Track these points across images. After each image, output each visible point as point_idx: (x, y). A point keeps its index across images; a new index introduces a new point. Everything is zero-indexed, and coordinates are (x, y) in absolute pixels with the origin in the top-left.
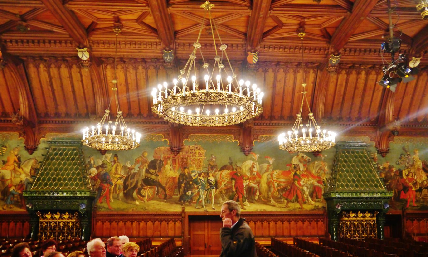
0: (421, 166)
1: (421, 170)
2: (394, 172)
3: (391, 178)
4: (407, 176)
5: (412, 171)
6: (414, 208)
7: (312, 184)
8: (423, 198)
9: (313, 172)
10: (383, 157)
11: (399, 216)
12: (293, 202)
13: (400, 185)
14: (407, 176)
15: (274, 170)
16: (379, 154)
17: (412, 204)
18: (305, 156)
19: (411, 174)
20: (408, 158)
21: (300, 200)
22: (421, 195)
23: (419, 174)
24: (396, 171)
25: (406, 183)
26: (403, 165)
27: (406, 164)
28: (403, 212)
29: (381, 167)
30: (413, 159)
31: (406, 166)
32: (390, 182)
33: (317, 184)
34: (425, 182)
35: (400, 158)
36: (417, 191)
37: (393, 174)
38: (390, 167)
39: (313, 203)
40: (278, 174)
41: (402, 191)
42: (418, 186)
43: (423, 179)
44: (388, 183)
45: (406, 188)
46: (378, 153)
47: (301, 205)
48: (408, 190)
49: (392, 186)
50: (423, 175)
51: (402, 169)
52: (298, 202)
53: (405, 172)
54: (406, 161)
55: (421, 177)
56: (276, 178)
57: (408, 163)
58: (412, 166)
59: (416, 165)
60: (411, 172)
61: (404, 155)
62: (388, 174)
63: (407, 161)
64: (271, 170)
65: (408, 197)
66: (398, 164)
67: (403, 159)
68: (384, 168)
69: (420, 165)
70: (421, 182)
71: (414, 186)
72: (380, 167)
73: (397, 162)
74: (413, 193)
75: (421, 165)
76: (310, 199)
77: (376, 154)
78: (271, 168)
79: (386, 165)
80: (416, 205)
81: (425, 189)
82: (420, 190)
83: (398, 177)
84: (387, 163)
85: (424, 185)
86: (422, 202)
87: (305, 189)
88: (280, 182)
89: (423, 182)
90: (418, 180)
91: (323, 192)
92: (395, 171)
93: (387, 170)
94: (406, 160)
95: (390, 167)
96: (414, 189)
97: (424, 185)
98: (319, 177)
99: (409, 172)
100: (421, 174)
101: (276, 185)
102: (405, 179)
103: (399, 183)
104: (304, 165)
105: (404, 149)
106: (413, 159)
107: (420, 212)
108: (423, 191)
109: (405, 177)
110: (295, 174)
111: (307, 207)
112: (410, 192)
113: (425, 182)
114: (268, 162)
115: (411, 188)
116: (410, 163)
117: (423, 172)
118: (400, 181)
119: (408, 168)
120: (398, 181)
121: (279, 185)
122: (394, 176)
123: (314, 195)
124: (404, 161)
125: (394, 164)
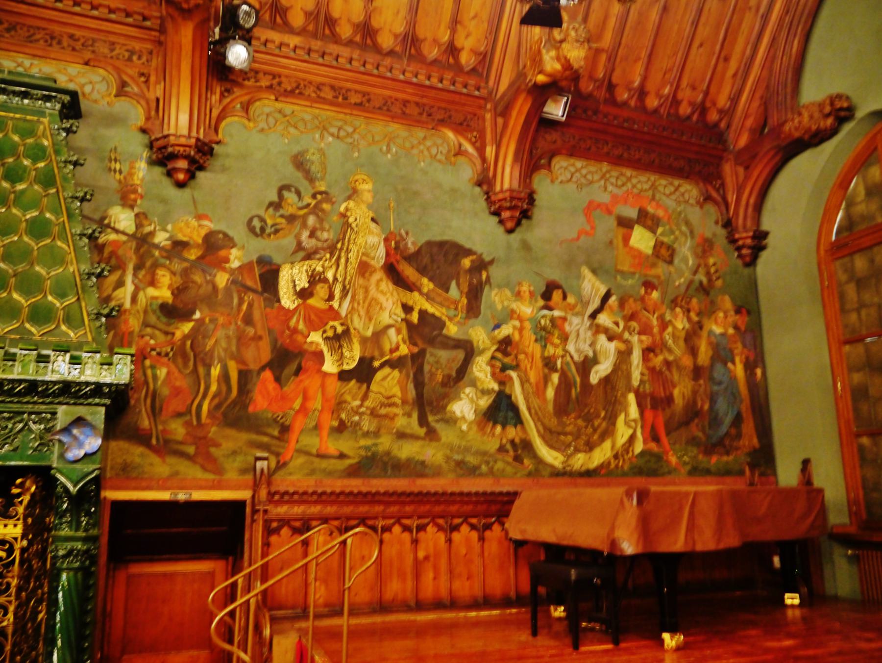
0: (379, 255)
1: (379, 275)
2: (232, 272)
3: (211, 298)
4: (304, 294)
5: (330, 275)
6: (324, 464)
8: (373, 413)
10: (181, 185)
11: (234, 511)
13: (258, 338)
14: (304, 294)
16: (158, 171)
17: (312, 442)
19: (321, 291)
20: (316, 210)
22: (365, 397)
23: (367, 291)
24: (246, 268)
25: (295, 331)
26: (288, 242)
27: (305, 234)
28: (256, 487)
29: (161, 238)
30: (344, 216)
31: (299, 247)
32: (201, 322)
34: (392, 332)
35: (276, 206)
36: (344, 376)
37: (222, 279)
38: (214, 246)
41: (268, 374)
42: (353, 355)
43: (385, 318)
44: (186, 327)
45: (288, 359)
46: (152, 163)
48: (298, 371)
49: (211, 343)
50: (382, 299)
51: (277, 259)
53: (292, 277)
54: (304, 225)
55: (371, 308)
57: (312, 235)
58: (332, 249)
59: (354, 249)
60: (326, 280)
61: (298, 193)
62: (198, 278)
63: (311, 220)
65: (297, 405)
66: (258, 231)
67: (289, 210)
68: (179, 246)
69: (375, 247)
70: (369, 333)
71: (332, 349)
72: (152, 234)
73: (256, 223)
74: (323, 386)
75: (381, 251)
77: (142, 165)
79: (193, 230)
80: (333, 446)
81: (387, 370)
82: (364, 372)
83: (249, 297)
84: (200, 217)
85: (387, 347)
86: (367, 434)
89: (379, 334)
90: (357, 323)
92: (235, 264)
93: (193, 255)
94: (304, 218)
95: (214, 246)
96: (330, 366)
97: (387, 347)
99: (315, 279)
100: (373, 292)
102: (289, 314)
103: (251, 331)
105: (299, 162)
106: (344, 216)
107: (356, 485)
108: (379, 375)
109: (288, 301)
112: (311, 382)
113: (392, 332)
115: (319, 357)
116: (325, 235)
117: (387, 285)
118: (257, 315)
119: (308, 257)
120: (248, 320)
122: (227, 289)
124: (291, 219)
125: (238, 233)
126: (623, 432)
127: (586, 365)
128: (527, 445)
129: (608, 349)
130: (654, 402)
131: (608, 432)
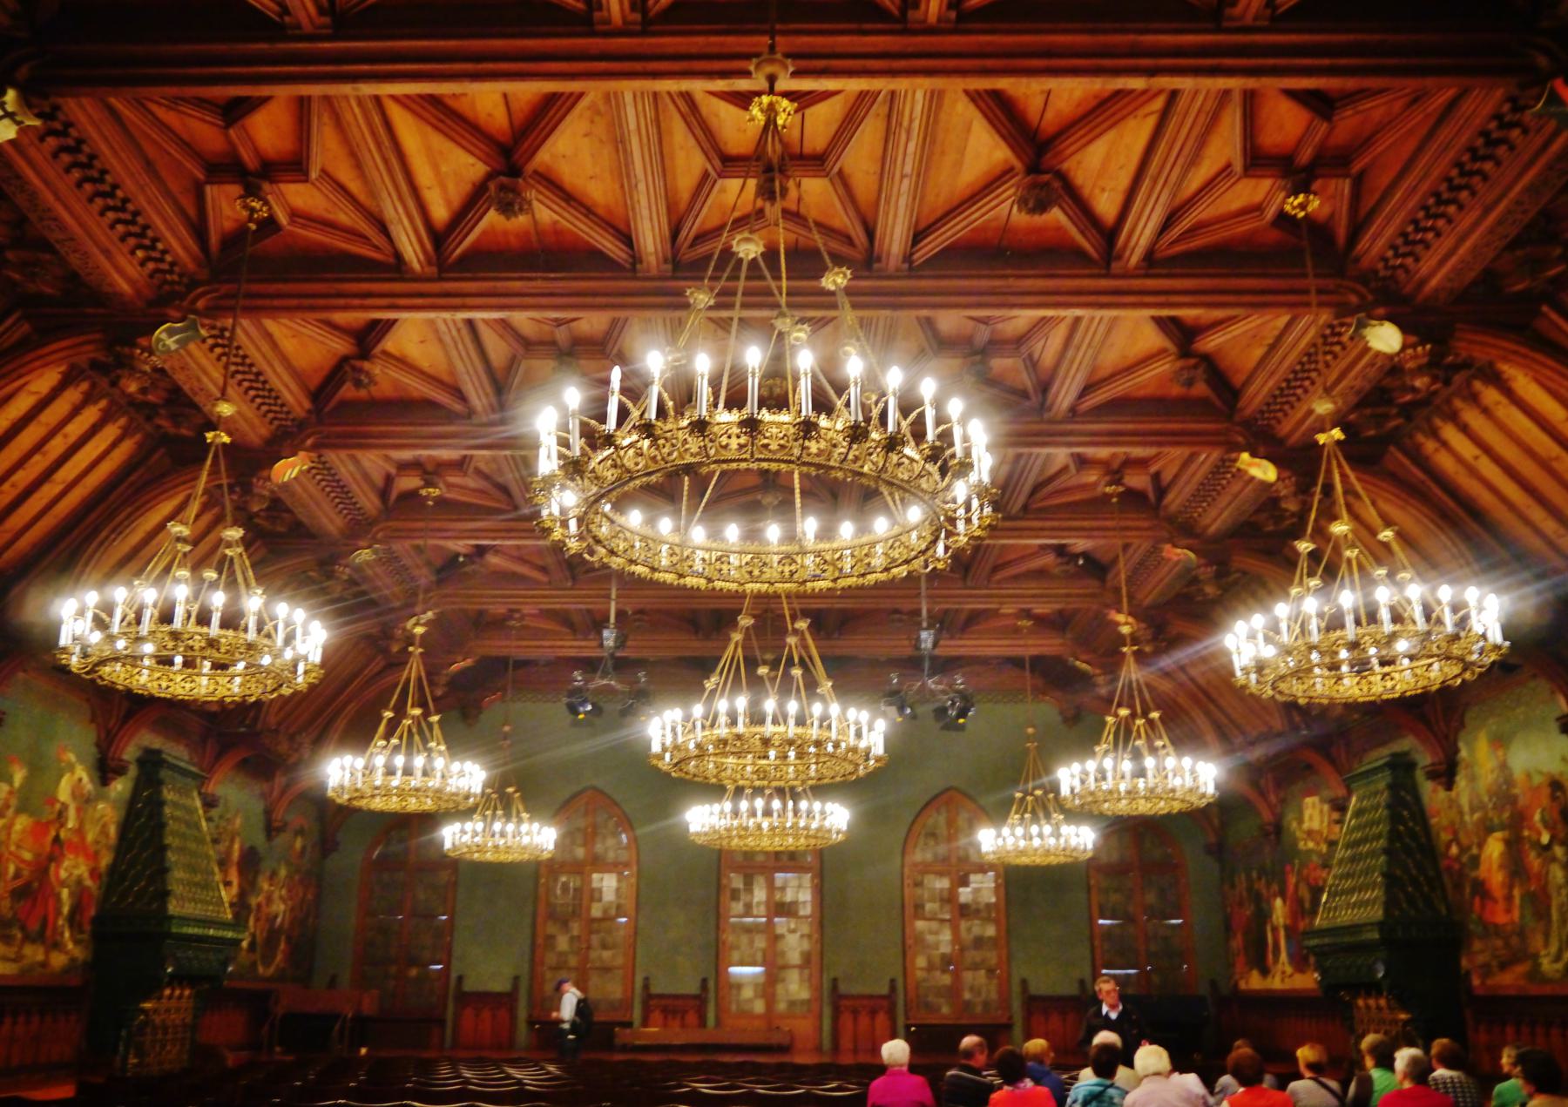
7: (79, 881)
9: (90, 837)
12: (33, 941)
15: (19, 811)
18: (86, 779)
21: (49, 932)
33: (88, 882)
39: (70, 946)
40: (24, 831)
47: (47, 953)
52: (43, 943)
56: (18, 847)
64: (10, 812)
76: (67, 935)
78: (14, 802)
87: (65, 893)
88: (23, 861)
91: (93, 912)
98: (94, 856)
101: (12, 869)
104: (79, 810)
110: (57, 839)
111: (58, 960)
114: (11, 783)
121: (17, 875)
123: (78, 917)
126: (279, 957)
127: (276, 917)
128: (254, 965)
129: (282, 907)
130: (289, 939)
131: (274, 957)
